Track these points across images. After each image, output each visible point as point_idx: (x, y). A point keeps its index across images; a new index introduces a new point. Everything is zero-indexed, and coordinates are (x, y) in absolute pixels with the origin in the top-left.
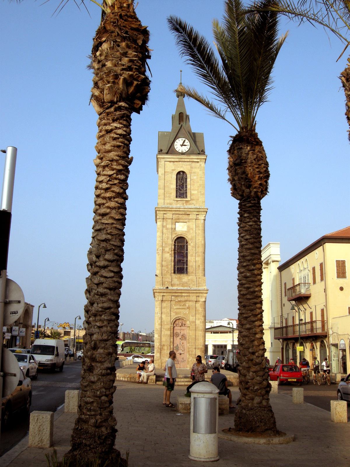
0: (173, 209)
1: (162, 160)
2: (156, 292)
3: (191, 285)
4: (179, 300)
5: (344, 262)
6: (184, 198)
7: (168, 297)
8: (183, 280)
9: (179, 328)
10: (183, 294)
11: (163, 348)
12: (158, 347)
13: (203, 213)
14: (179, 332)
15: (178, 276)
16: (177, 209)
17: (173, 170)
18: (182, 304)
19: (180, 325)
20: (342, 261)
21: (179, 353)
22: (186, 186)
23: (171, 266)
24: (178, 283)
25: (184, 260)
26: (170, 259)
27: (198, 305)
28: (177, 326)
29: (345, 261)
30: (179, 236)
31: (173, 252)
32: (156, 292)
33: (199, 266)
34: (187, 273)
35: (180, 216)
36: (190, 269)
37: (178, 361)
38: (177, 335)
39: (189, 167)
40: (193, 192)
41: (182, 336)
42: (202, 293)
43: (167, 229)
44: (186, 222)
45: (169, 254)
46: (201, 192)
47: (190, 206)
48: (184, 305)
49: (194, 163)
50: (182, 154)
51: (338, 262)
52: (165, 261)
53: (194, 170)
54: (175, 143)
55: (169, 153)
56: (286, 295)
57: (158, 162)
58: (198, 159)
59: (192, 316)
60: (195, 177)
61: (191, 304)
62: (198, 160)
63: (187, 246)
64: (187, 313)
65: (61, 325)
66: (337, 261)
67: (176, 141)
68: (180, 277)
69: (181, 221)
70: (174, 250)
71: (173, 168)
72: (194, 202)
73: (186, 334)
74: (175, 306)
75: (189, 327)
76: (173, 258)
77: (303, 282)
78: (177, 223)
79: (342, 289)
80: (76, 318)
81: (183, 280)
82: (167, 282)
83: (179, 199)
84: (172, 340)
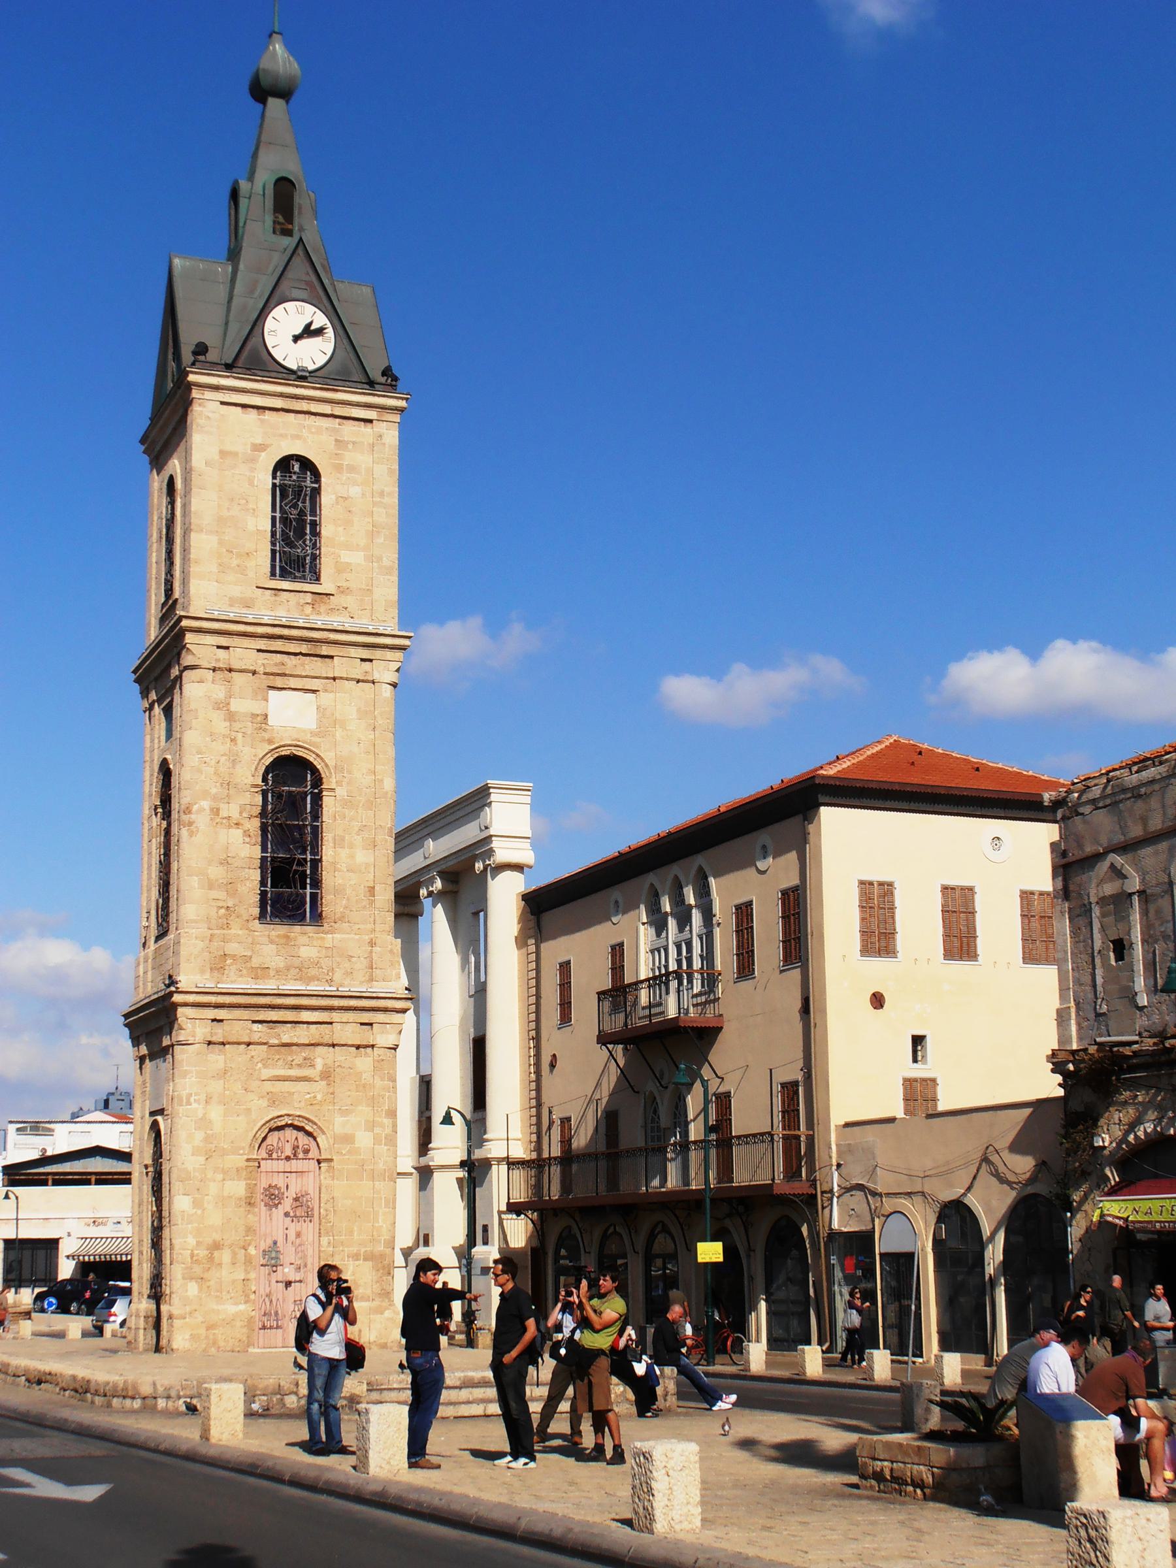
0: (260, 630)
1: (209, 395)
2: (186, 1005)
3: (338, 976)
4: (286, 1039)
5: (887, 889)
6: (304, 577)
9: (281, 1165)
10: (306, 1016)
11: (211, 1259)
12: (192, 1256)
13: (389, 655)
14: (279, 1181)
15: (279, 930)
16: (277, 631)
17: (259, 448)
18: (298, 1059)
19: (288, 1151)
20: (881, 884)
21: (280, 1279)
22: (314, 524)
23: (251, 881)
24: (277, 962)
25: (302, 862)
27: (364, 1062)
28: (274, 1156)
29: (891, 884)
30: (285, 752)
31: (257, 823)
32: (186, 1005)
33: (372, 890)
34: (317, 917)
35: (291, 661)
36: (330, 904)
38: (273, 1197)
39: (328, 441)
40: (346, 557)
41: (296, 1199)
42: (385, 1010)
43: (231, 717)
44: (314, 691)
45: (237, 833)
46: (380, 559)
47: (336, 621)
48: (309, 1062)
49: (351, 422)
50: (303, 378)
51: (865, 886)
52: (225, 862)
53: (350, 457)
54: (270, 324)
55: (240, 363)
56: (565, 1017)
57: (187, 403)
59: (344, 1113)
60: (355, 491)
61: (339, 1054)
62: (371, 414)
63: (318, 799)
64: (319, 1097)
66: (865, 886)
68: (287, 937)
69: (293, 683)
70: (263, 814)
71: (259, 441)
72: (349, 601)
73: (311, 1191)
74: (265, 1066)
75: (331, 1160)
76: (257, 852)
77: (673, 966)
78: (271, 692)
79: (878, 1001)
82: (234, 957)
83: (285, 585)
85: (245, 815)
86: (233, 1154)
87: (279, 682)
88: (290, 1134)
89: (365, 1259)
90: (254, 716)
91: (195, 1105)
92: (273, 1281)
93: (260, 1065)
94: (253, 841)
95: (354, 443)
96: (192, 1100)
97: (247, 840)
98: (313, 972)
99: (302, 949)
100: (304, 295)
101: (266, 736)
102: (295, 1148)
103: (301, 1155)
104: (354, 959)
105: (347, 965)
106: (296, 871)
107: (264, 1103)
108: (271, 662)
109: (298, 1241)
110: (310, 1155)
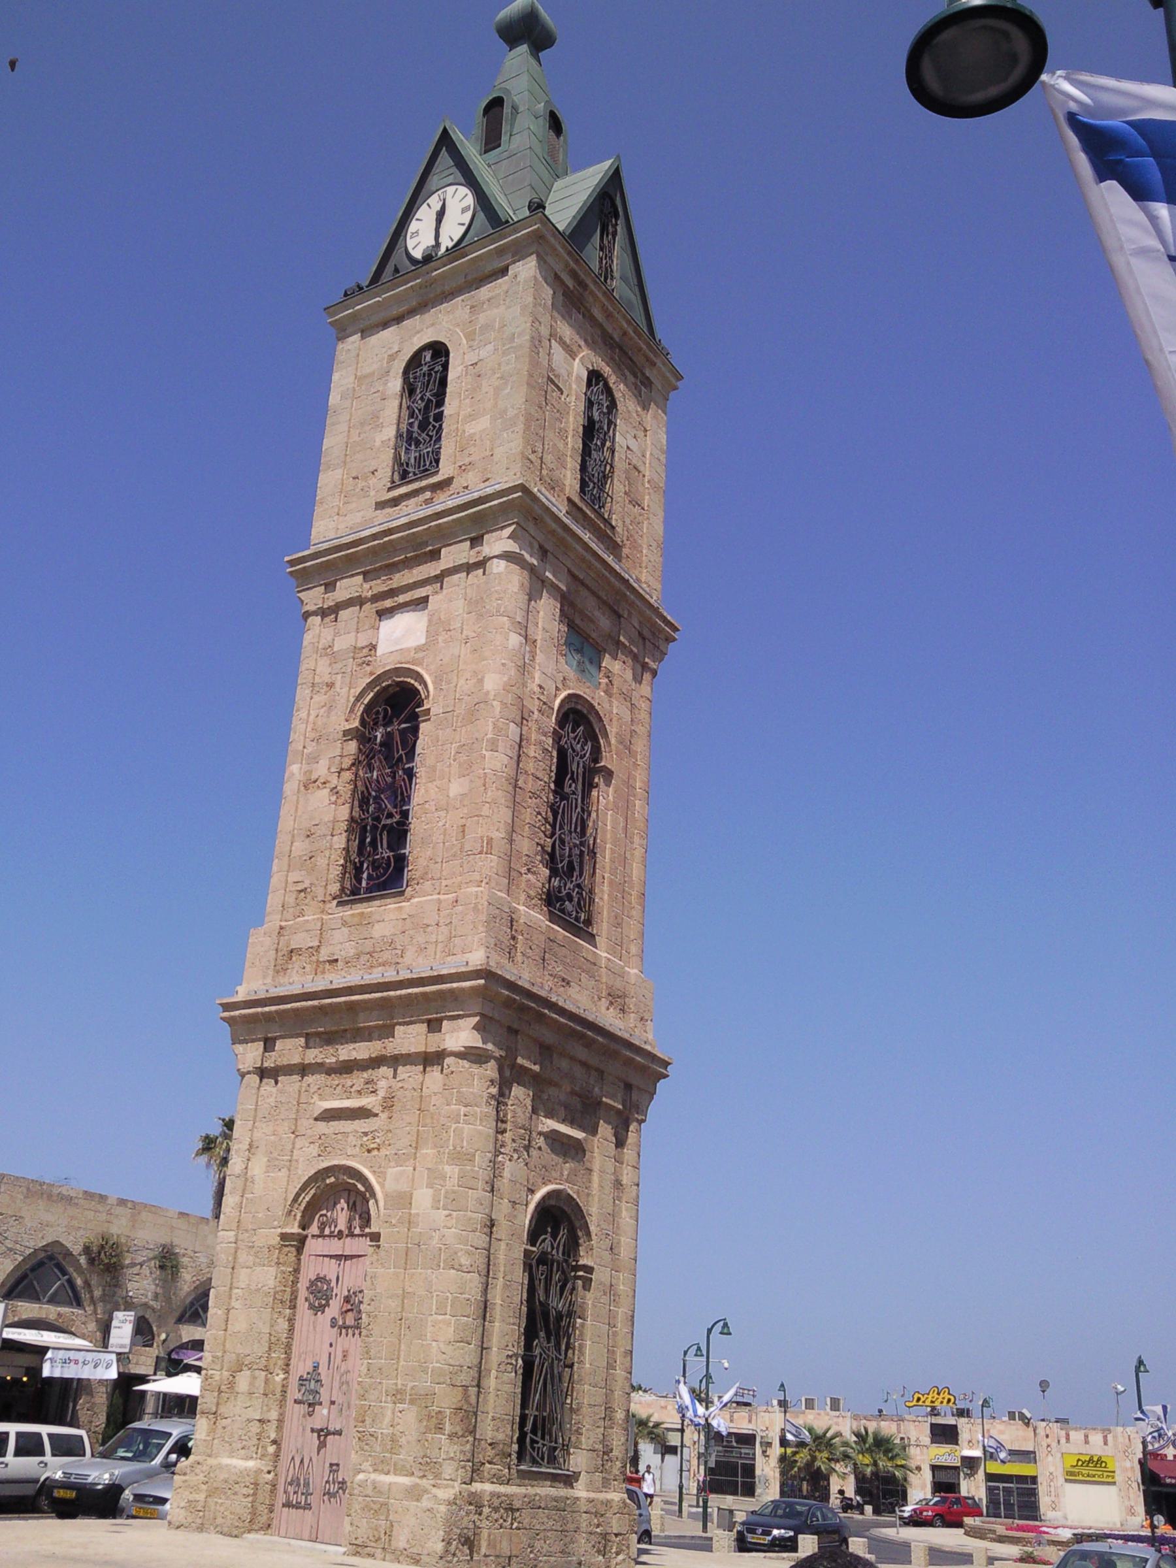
6: (425, 473)
7: (290, 1050)
8: (379, 931)
9: (335, 1246)
14: (330, 1269)
17: (392, 358)
24: (349, 950)
26: (327, 817)
28: (327, 1232)
40: (472, 428)
41: (347, 1300)
46: (505, 411)
53: (482, 318)
54: (413, 226)
58: (500, 252)
65: (919, 1399)
69: (402, 599)
74: (322, 1098)
80: (709, 1331)
81: (378, 931)
87: (388, 603)
88: (337, 1195)
94: (340, 801)
98: (386, 956)
100: (451, 179)
105: (420, 938)
106: (385, 826)
107: (314, 1150)
108: (379, 586)
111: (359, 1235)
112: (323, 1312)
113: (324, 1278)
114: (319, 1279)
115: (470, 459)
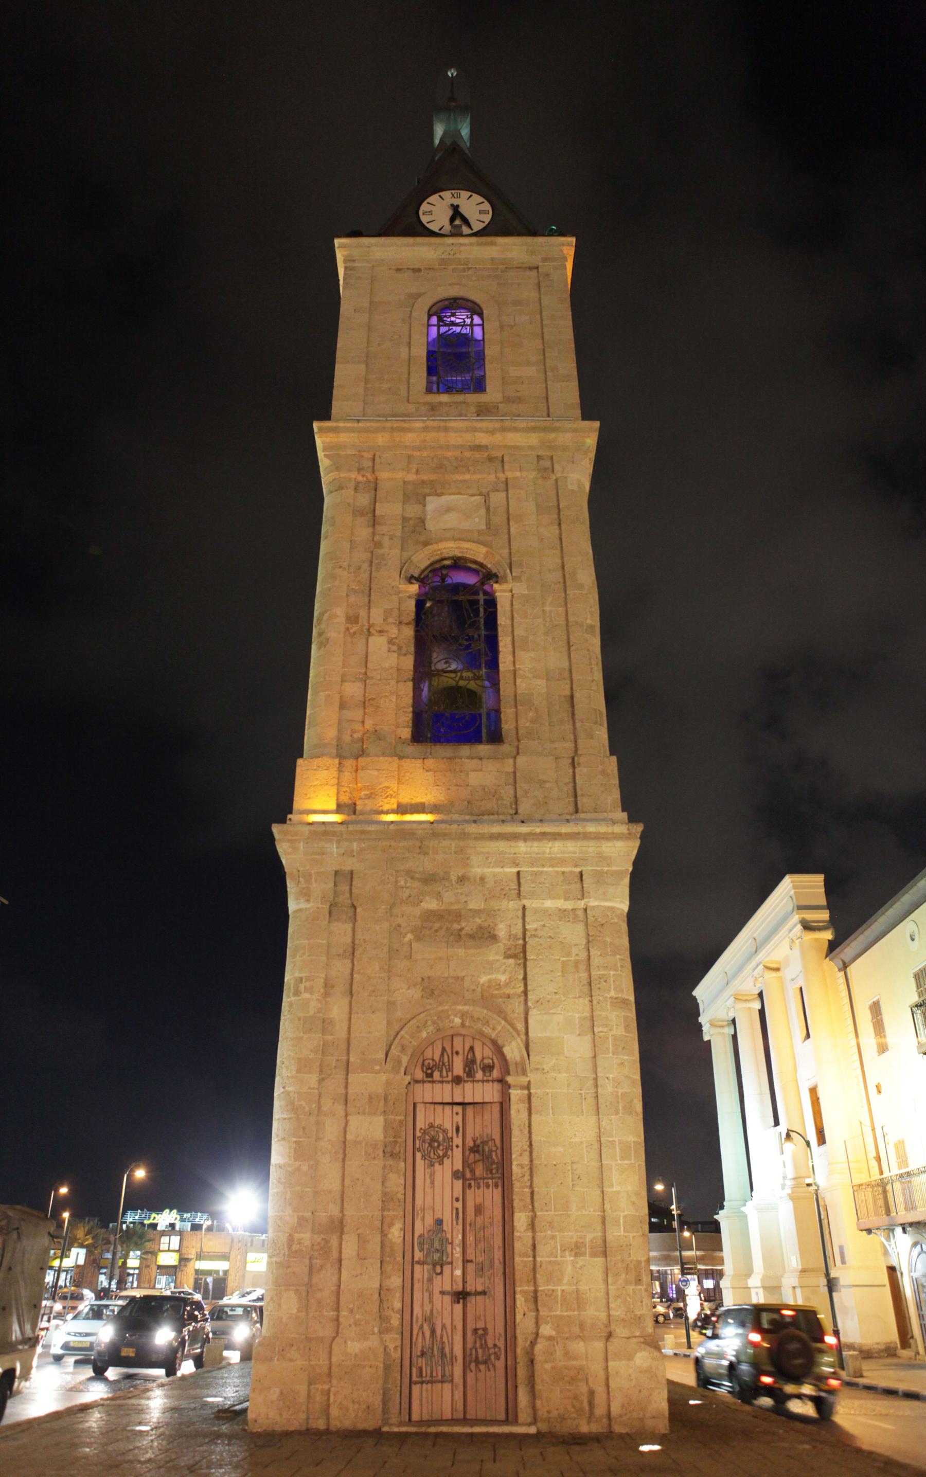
14: (447, 1119)
19: (458, 1068)
21: (447, 1288)
28: (436, 1075)
34: (496, 737)
37: (443, 1355)
38: (433, 1145)
40: (514, 372)
41: (475, 1149)
67: (430, 200)
71: (414, 290)
76: (408, 662)
83: (444, 398)
84: (396, 1182)
85: (390, 620)
86: (363, 1071)
89: (594, 1255)
90: (405, 519)
91: (306, 996)
92: (437, 1297)
93: (410, 936)
95: (519, 284)
96: (302, 987)
97: (395, 648)
98: (490, 805)
99: (472, 775)
101: (422, 538)
102: (470, 1064)
103: (479, 1075)
104: (548, 785)
109: (479, 1220)
110: (496, 1074)
111: (483, 1081)
112: (441, 1163)
113: (439, 1127)
114: (431, 1126)
115: (518, 394)
